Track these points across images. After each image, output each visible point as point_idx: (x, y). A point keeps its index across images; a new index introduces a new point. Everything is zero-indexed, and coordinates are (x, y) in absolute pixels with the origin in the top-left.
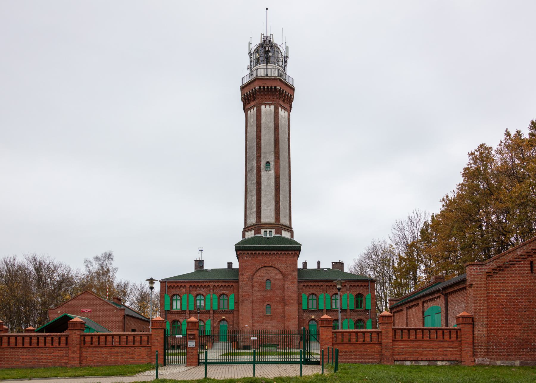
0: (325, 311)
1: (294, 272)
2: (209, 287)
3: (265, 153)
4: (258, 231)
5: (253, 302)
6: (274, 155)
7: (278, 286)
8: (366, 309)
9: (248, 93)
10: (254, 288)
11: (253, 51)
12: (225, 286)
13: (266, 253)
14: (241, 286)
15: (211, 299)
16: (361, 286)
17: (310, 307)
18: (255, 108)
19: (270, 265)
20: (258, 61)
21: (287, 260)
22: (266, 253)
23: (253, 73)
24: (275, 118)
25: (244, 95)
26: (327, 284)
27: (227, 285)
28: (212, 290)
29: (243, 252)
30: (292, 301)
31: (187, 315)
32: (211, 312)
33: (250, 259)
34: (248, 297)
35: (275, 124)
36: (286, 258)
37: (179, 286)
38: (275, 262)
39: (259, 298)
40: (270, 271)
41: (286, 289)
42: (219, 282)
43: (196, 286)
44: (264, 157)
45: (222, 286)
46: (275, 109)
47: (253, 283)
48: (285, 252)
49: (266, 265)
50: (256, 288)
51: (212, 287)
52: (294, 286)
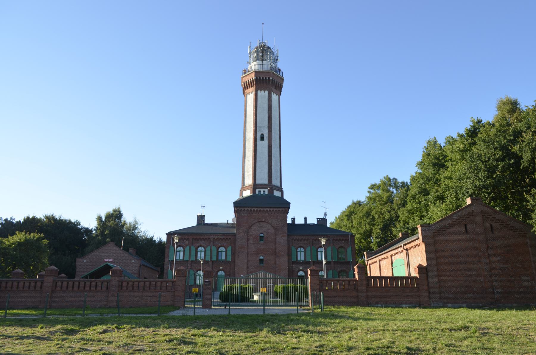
0: (312, 263)
1: (284, 227)
2: (209, 240)
3: (260, 127)
4: (254, 191)
5: (248, 254)
6: (267, 129)
7: (271, 240)
8: (348, 261)
10: (249, 241)
12: (224, 238)
13: (260, 210)
14: (238, 239)
15: (211, 251)
16: (343, 239)
17: (299, 259)
19: (264, 220)
21: (278, 216)
22: (260, 210)
24: (268, 100)
26: (313, 238)
27: (225, 238)
28: (212, 243)
29: (241, 209)
30: (283, 253)
31: (189, 266)
32: (211, 263)
33: (246, 215)
34: (244, 249)
35: (268, 105)
36: (277, 215)
37: (183, 238)
38: (268, 218)
39: (254, 250)
40: (263, 226)
41: (278, 242)
42: (219, 235)
43: (198, 238)
44: (259, 130)
45: (221, 238)
46: (268, 94)
47: (248, 237)
48: (277, 209)
49: (260, 220)
50: (251, 241)
51: (212, 240)
52: (284, 239)
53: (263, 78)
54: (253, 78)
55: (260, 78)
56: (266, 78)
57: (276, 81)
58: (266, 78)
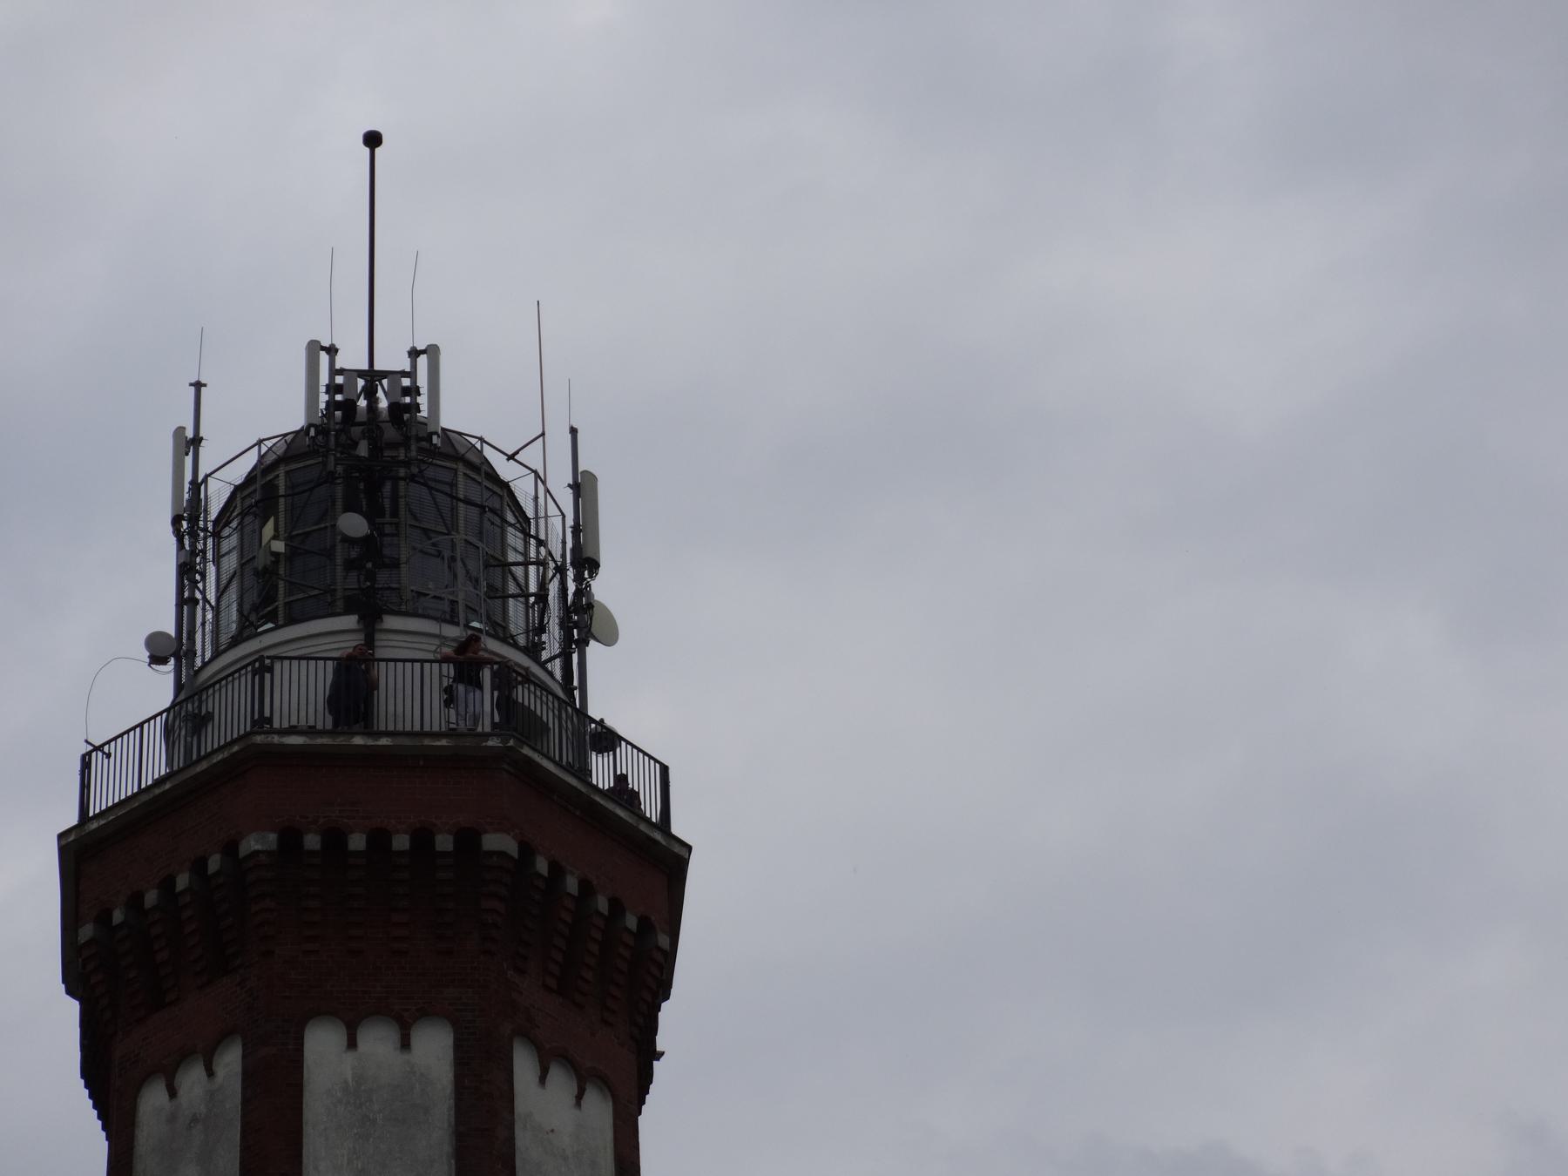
9: (151, 898)
11: (217, 495)
18: (230, 1060)
20: (268, 597)
23: (214, 703)
25: (104, 918)
53: (378, 838)
54: (230, 848)
55: (335, 838)
56: (423, 838)
57: (572, 884)
58: (423, 838)
